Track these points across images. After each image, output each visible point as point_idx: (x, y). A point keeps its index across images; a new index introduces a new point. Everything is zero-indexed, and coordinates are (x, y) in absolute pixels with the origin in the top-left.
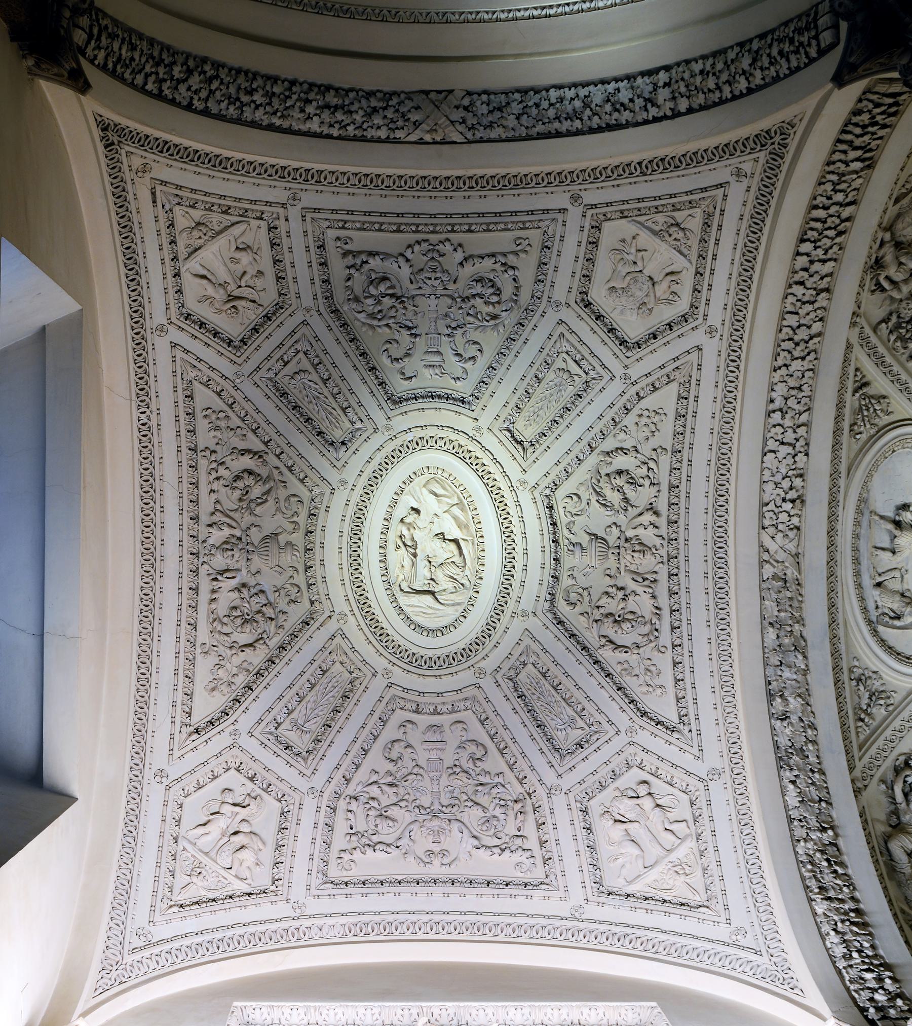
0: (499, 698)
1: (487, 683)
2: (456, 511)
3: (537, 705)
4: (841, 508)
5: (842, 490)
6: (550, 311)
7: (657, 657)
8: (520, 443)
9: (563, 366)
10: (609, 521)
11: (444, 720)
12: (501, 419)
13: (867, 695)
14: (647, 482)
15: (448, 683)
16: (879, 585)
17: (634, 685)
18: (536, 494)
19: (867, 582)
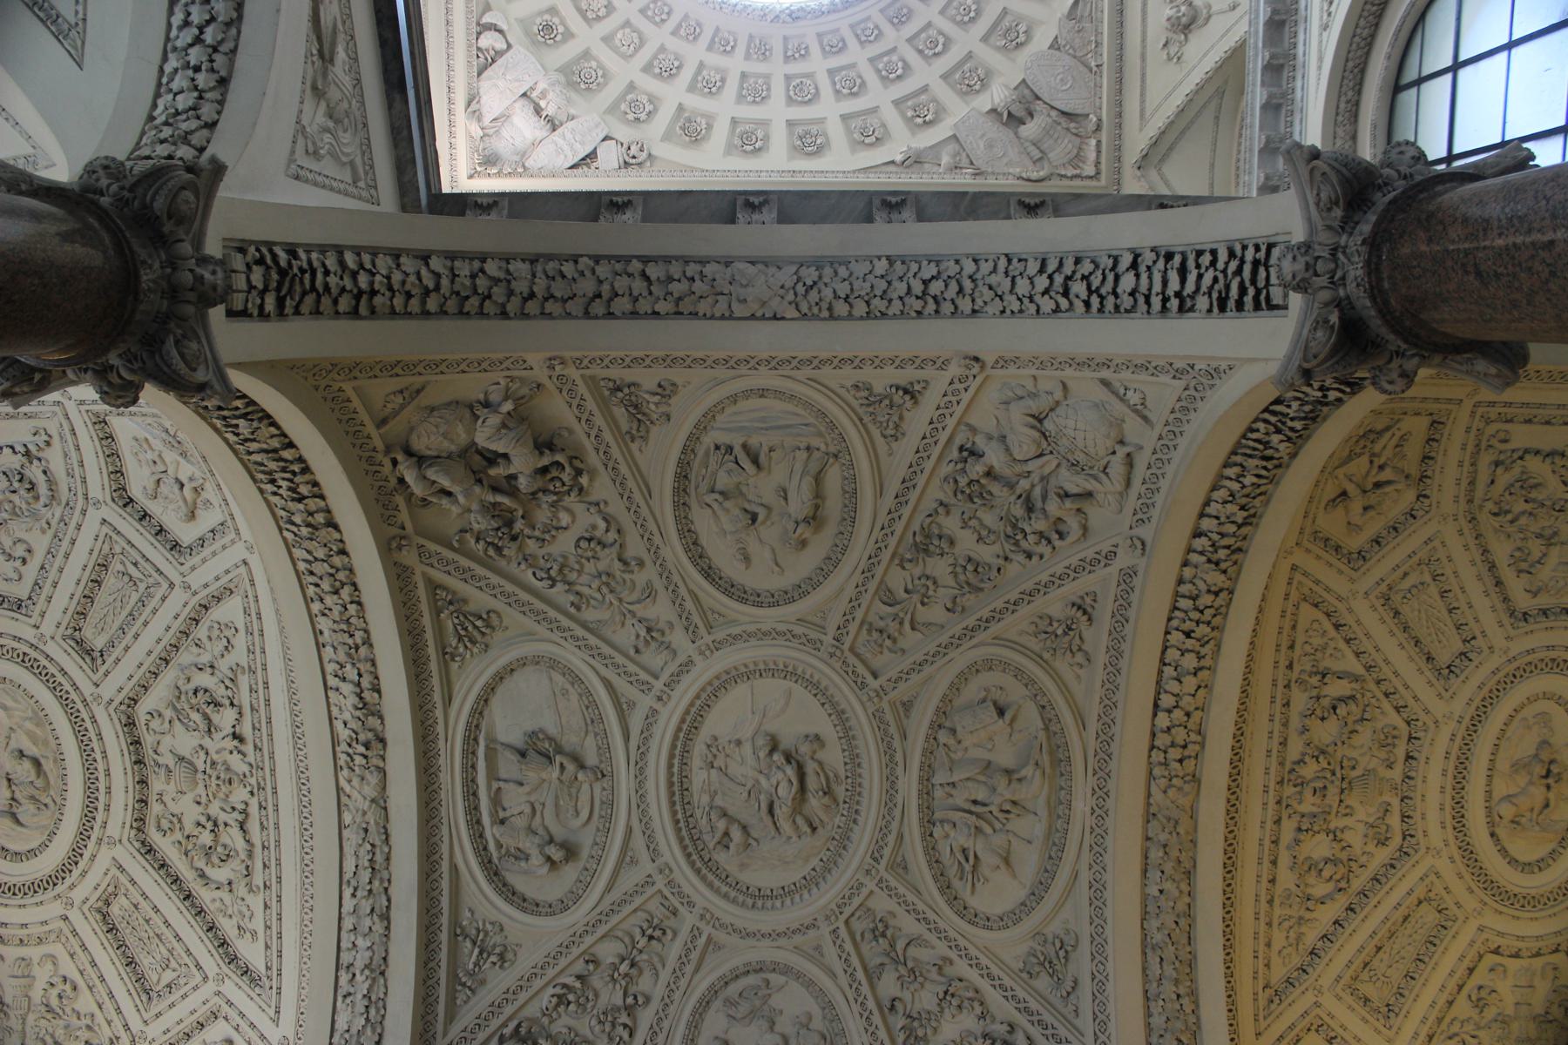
0: (89, 930)
1: (74, 915)
2: (29, 725)
3: (131, 940)
4: (441, 743)
5: (441, 721)
6: (91, 510)
7: (250, 899)
8: (89, 652)
9: (121, 568)
10: (196, 743)
11: (34, 952)
12: (63, 627)
13: (476, 951)
14: (227, 702)
15: (32, 915)
16: (502, 822)
17: (228, 927)
18: (111, 709)
19: (486, 820)
